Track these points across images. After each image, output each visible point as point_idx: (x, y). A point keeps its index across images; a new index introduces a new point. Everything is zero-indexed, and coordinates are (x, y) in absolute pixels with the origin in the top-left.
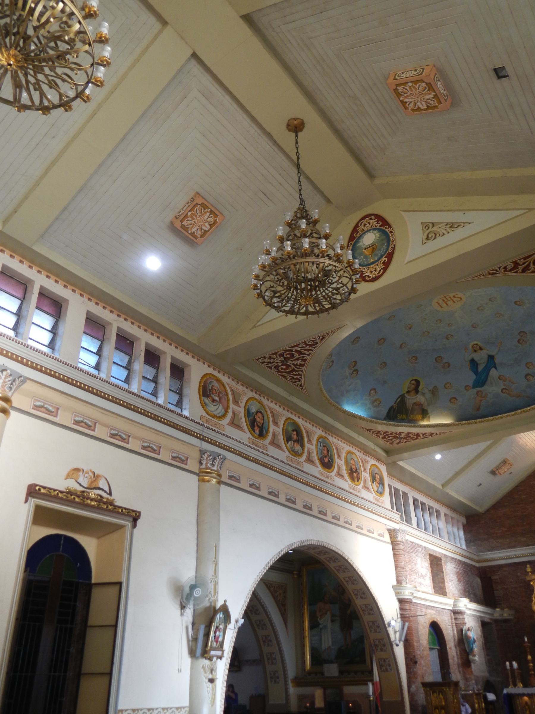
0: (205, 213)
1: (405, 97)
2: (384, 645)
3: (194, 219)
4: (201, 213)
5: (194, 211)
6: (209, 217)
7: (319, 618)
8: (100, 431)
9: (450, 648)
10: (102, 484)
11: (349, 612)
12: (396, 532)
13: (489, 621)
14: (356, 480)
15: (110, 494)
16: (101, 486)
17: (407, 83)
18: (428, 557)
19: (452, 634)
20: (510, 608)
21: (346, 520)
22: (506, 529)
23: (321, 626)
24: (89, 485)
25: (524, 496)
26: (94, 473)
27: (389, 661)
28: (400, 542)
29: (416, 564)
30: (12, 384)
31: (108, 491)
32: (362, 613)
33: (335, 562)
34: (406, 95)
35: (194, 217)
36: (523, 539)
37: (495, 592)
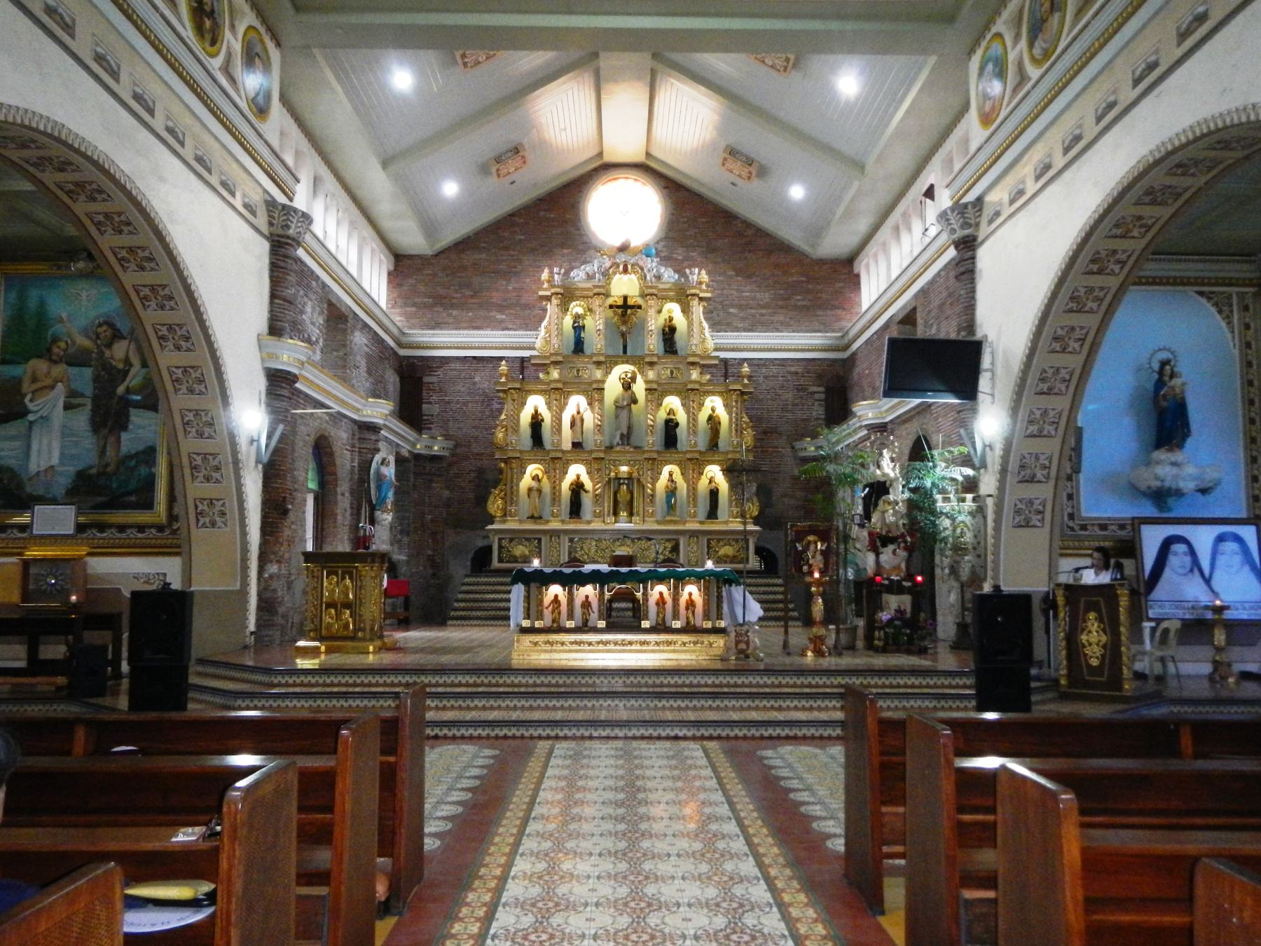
2: (217, 469)
7: (29, 397)
9: (343, 494)
12: (288, 214)
13: (407, 455)
14: (208, 37)
18: (326, 306)
19: (349, 467)
20: (447, 437)
21: (170, 124)
22: (472, 293)
23: (31, 417)
25: (522, 237)
27: (223, 505)
28: (293, 239)
29: (302, 312)
32: (169, 387)
33: (121, 232)
36: (499, 316)
37: (424, 406)
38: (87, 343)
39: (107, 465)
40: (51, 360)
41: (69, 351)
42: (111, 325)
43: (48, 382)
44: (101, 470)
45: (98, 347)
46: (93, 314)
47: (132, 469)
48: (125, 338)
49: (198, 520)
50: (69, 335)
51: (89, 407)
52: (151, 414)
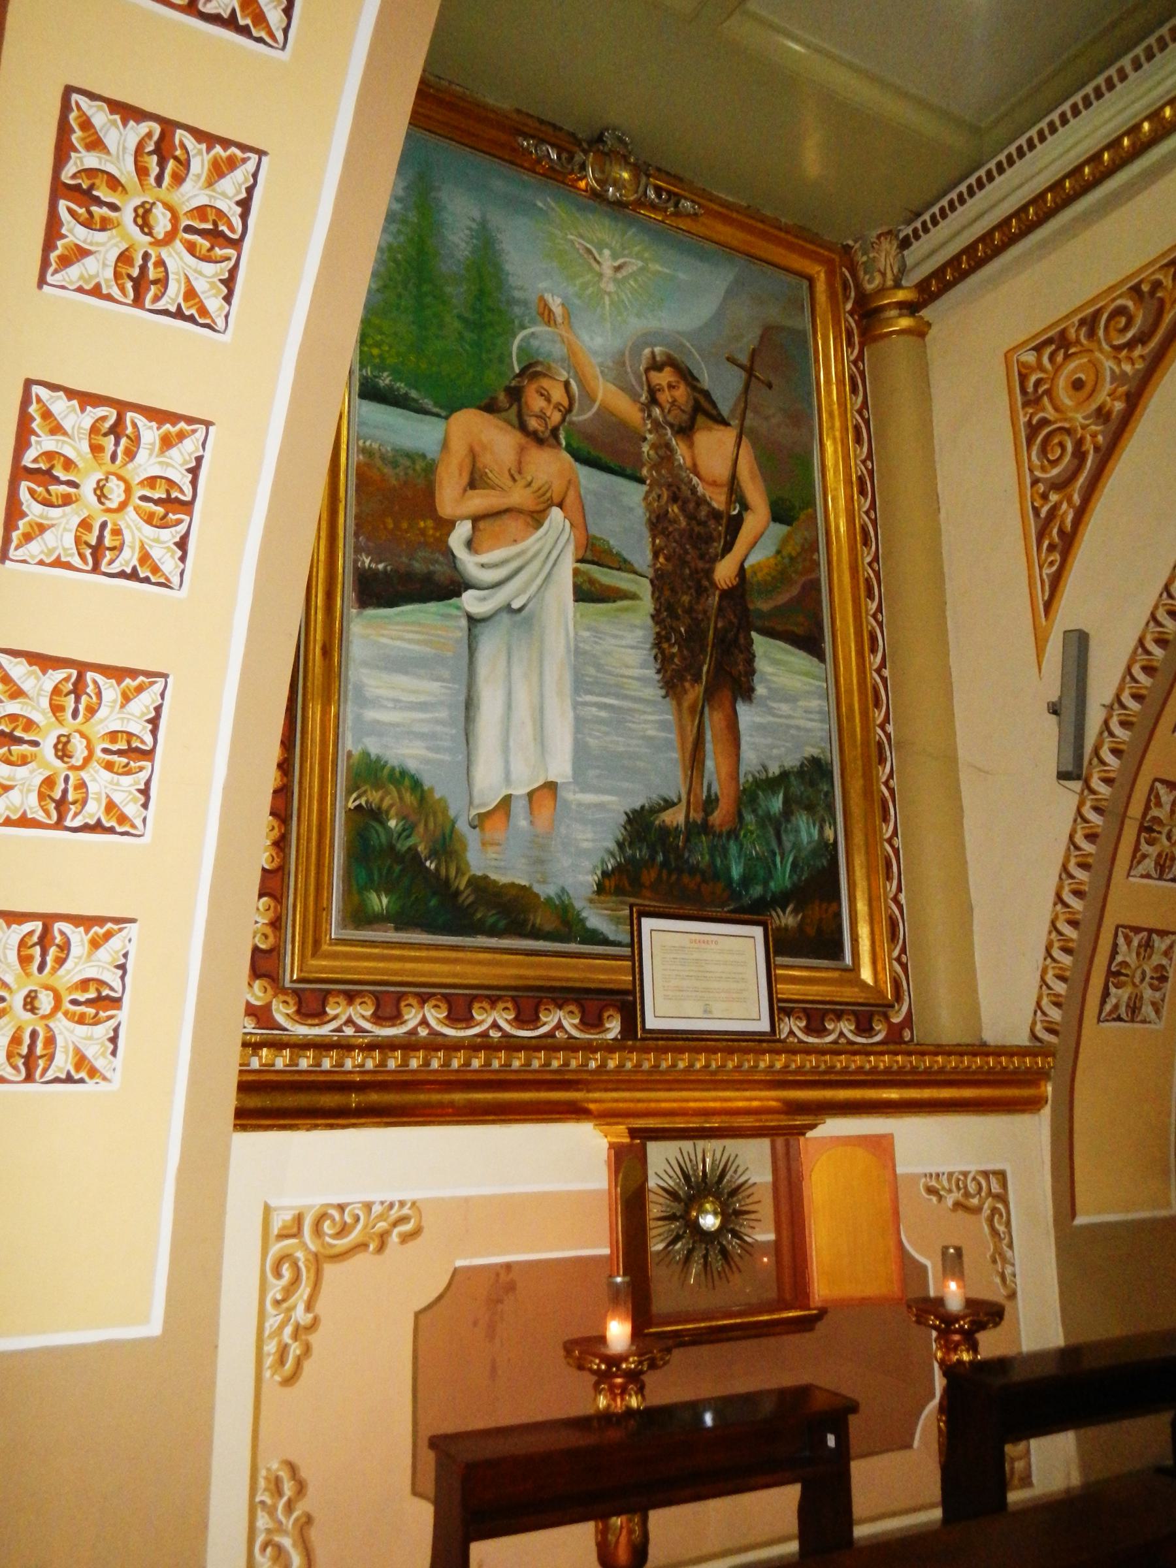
7: (463, 530)
11: (725, 572)
23: (470, 601)
38: (628, 409)
39: (710, 803)
40: (523, 427)
41: (575, 417)
42: (687, 376)
43: (519, 496)
44: (697, 816)
45: (657, 426)
46: (636, 325)
47: (778, 825)
48: (725, 423)
49: (1106, 994)
50: (571, 361)
51: (647, 604)
52: (800, 659)
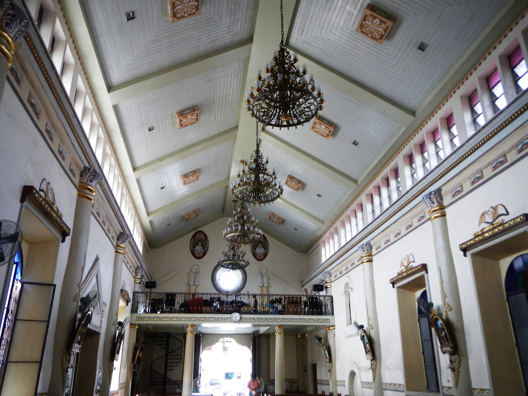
0: (366, 24)
1: (194, 5)
3: (373, 32)
4: (367, 27)
5: (367, 33)
6: (369, 21)
8: (488, 173)
10: (501, 211)
15: (508, 214)
16: (500, 213)
17: (188, 16)
24: (493, 219)
26: (493, 207)
30: (431, 200)
31: (505, 213)
34: (193, 7)
35: (371, 32)
